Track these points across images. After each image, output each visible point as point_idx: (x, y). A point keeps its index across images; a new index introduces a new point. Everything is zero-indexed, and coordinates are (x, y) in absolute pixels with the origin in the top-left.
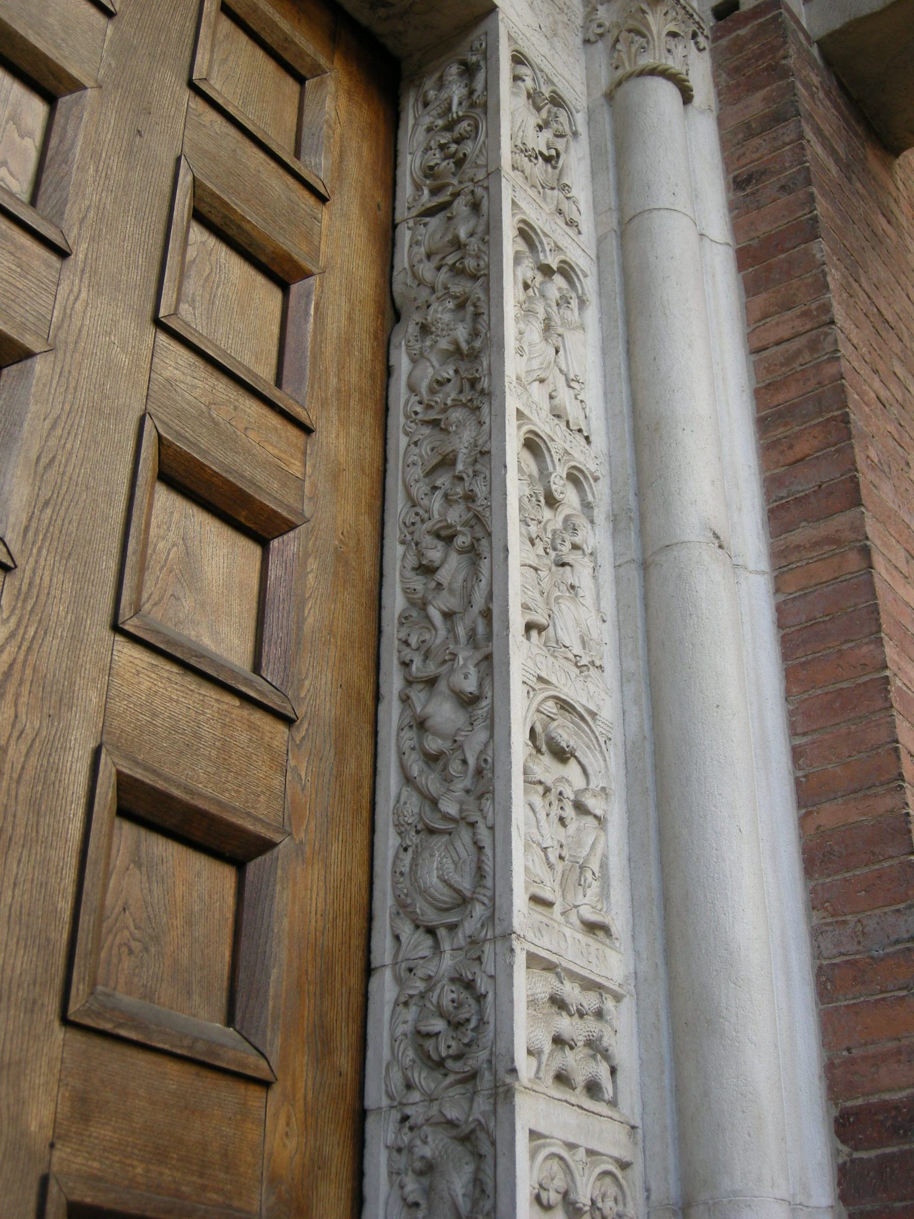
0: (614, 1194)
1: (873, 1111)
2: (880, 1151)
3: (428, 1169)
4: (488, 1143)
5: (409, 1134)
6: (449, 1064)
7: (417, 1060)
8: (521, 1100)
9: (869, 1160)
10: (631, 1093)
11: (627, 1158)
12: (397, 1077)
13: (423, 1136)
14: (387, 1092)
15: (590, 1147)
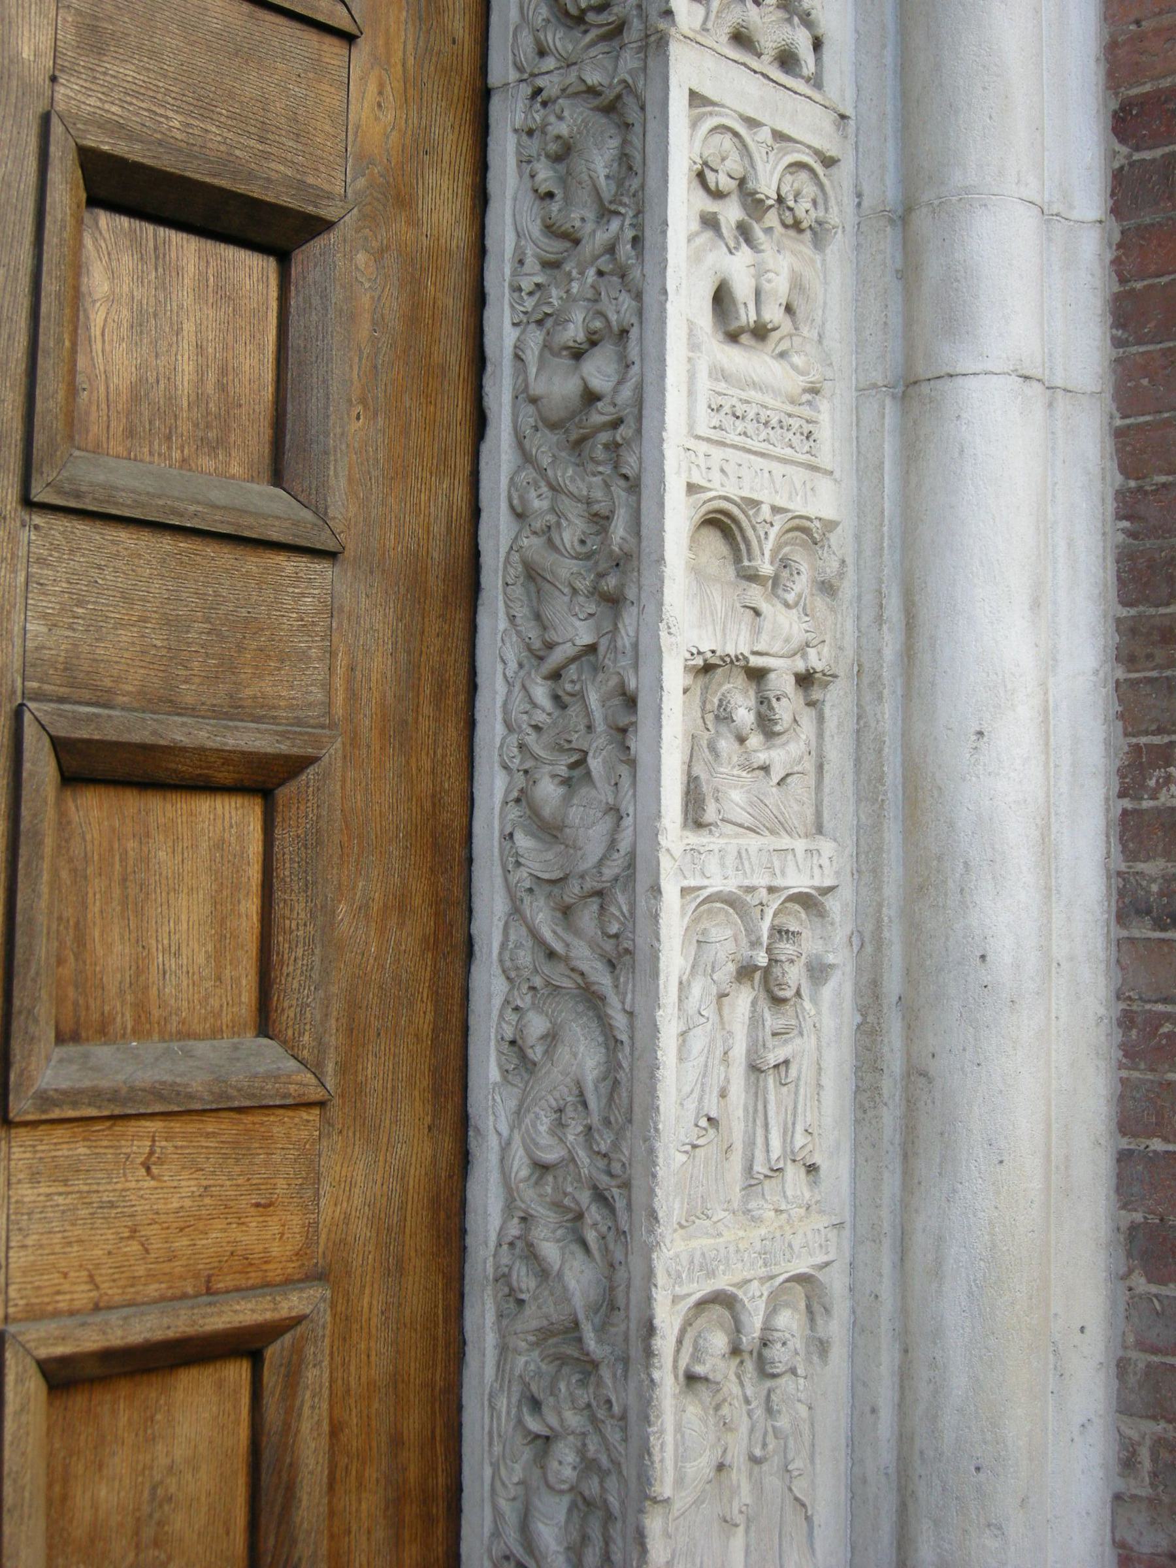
0: (812, 195)
1: (1163, 98)
2: (1167, 149)
3: (563, 153)
4: (636, 108)
5: (542, 111)
6: (591, 17)
7: (553, 20)
8: (675, 49)
9: (1154, 160)
10: (841, 73)
11: (833, 152)
12: (526, 41)
13: (558, 111)
14: (515, 64)
15: (779, 128)
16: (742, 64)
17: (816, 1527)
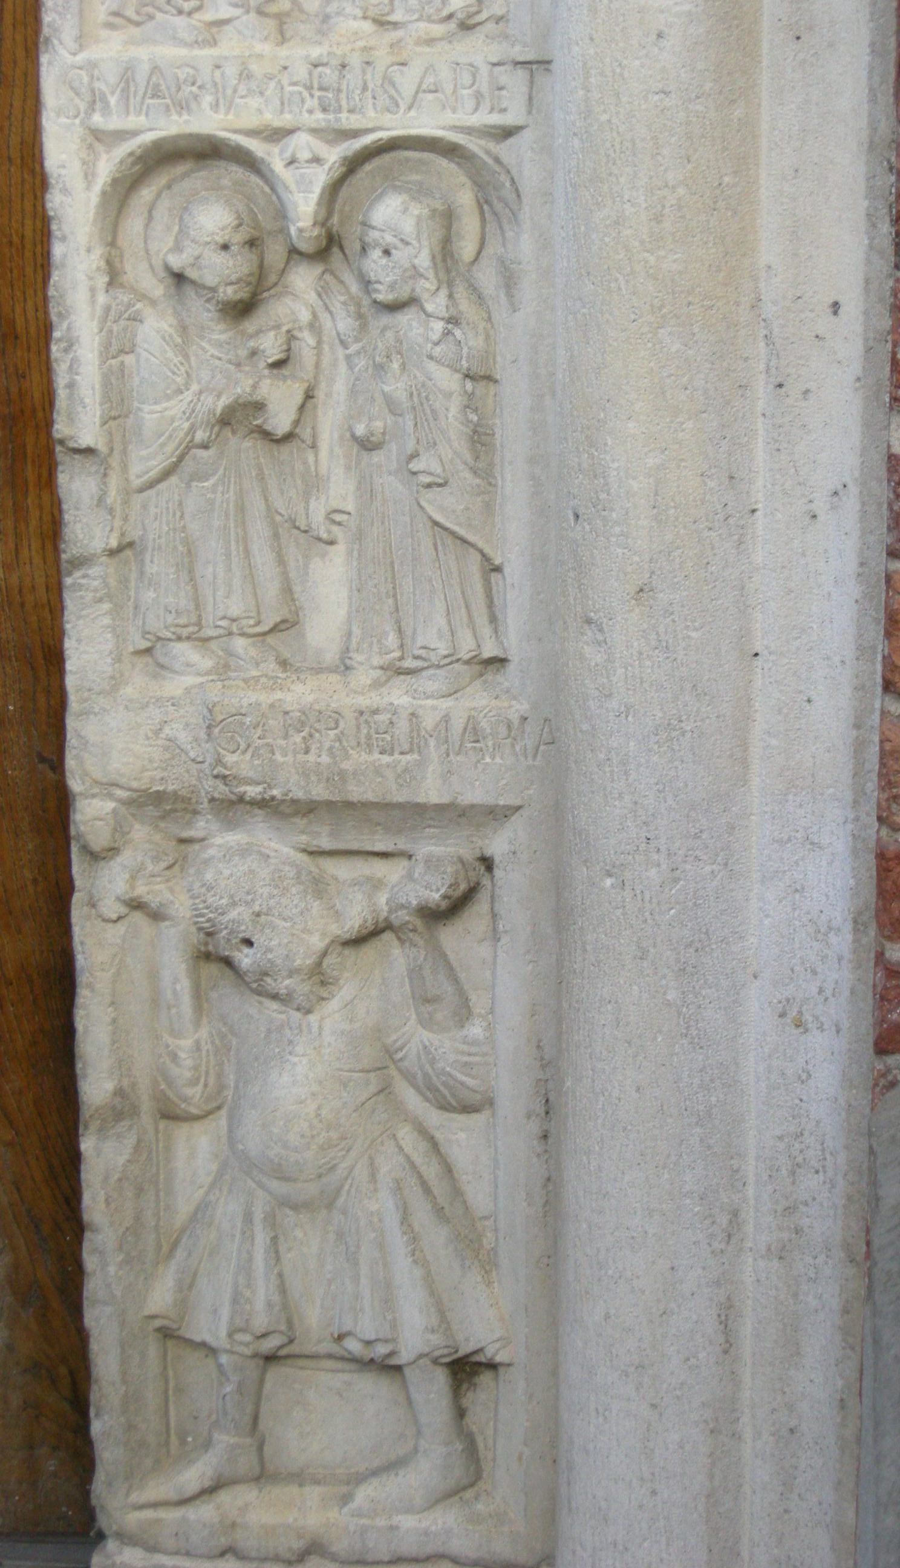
17: (508, 588)
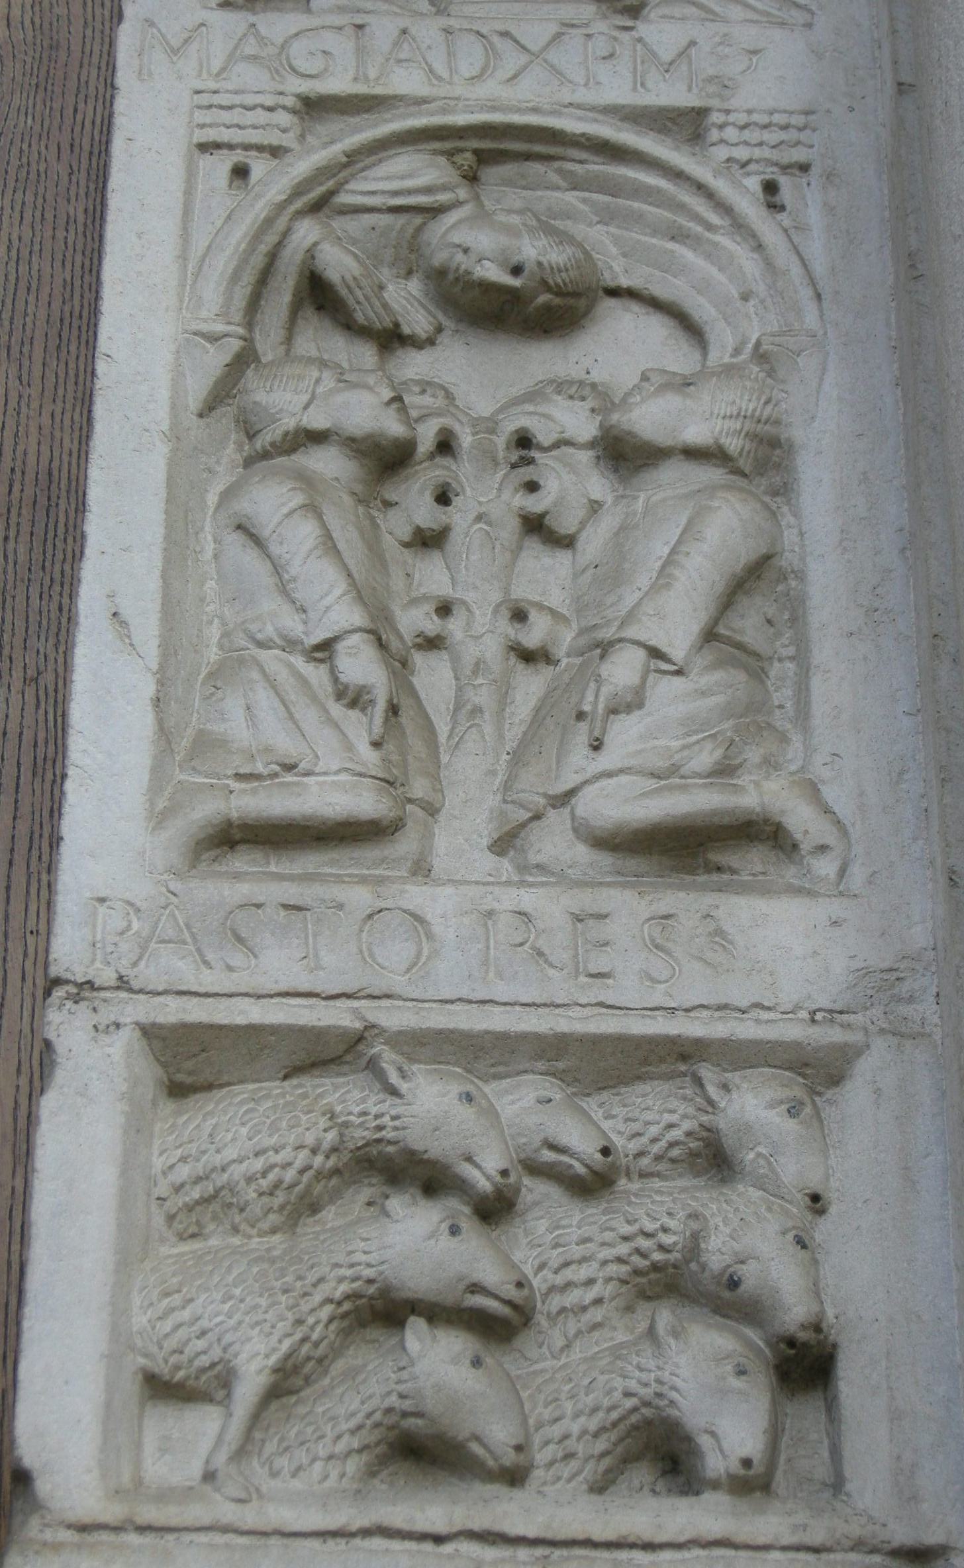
16: (366, 1533)
